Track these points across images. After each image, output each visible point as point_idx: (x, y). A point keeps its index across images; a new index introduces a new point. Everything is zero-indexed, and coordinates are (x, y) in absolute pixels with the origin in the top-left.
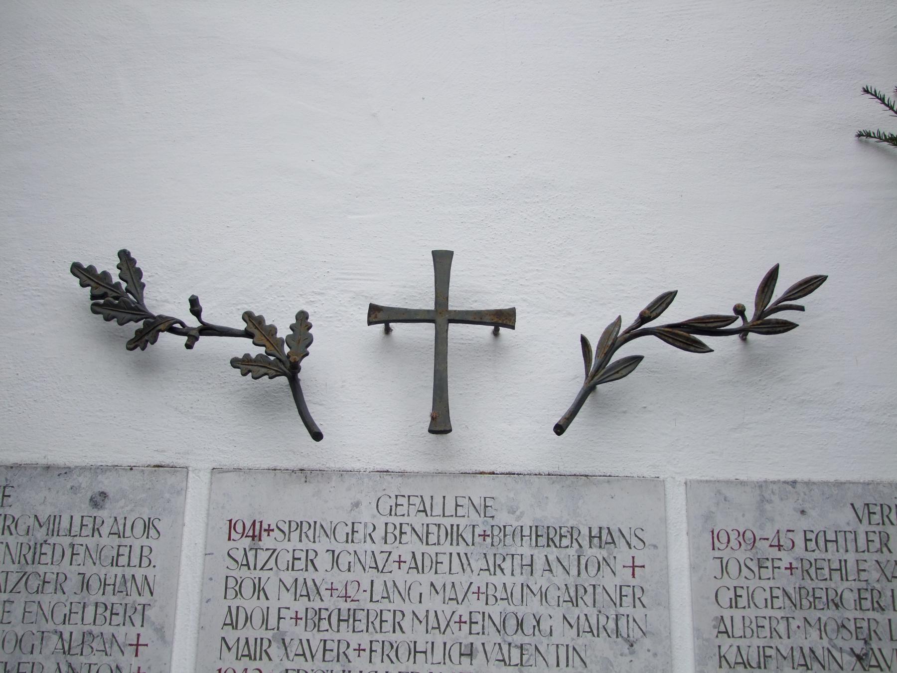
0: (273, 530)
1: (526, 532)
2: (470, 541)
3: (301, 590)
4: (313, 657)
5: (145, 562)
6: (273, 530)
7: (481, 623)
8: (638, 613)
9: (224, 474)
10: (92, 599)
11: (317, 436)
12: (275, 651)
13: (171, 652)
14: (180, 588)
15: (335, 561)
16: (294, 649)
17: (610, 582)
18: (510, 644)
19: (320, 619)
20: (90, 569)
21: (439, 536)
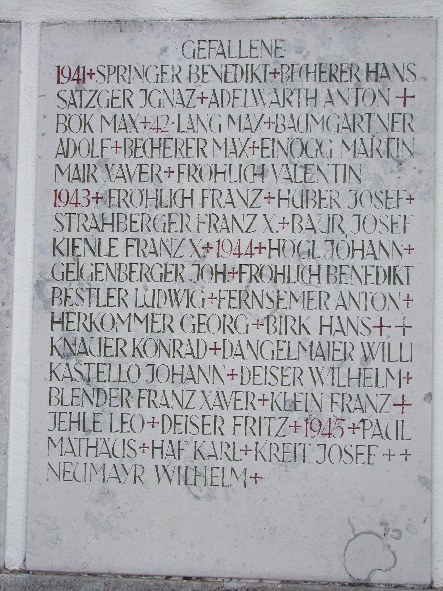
0: (94, 74)
1: (312, 69)
2: (262, 78)
4: (131, 179)
6: (94, 74)
7: (271, 148)
8: (407, 137)
9: (52, 27)
12: (100, 174)
13: (16, 178)
14: (20, 124)
15: (148, 99)
16: (115, 173)
18: (295, 165)
19: (136, 147)
21: (235, 75)
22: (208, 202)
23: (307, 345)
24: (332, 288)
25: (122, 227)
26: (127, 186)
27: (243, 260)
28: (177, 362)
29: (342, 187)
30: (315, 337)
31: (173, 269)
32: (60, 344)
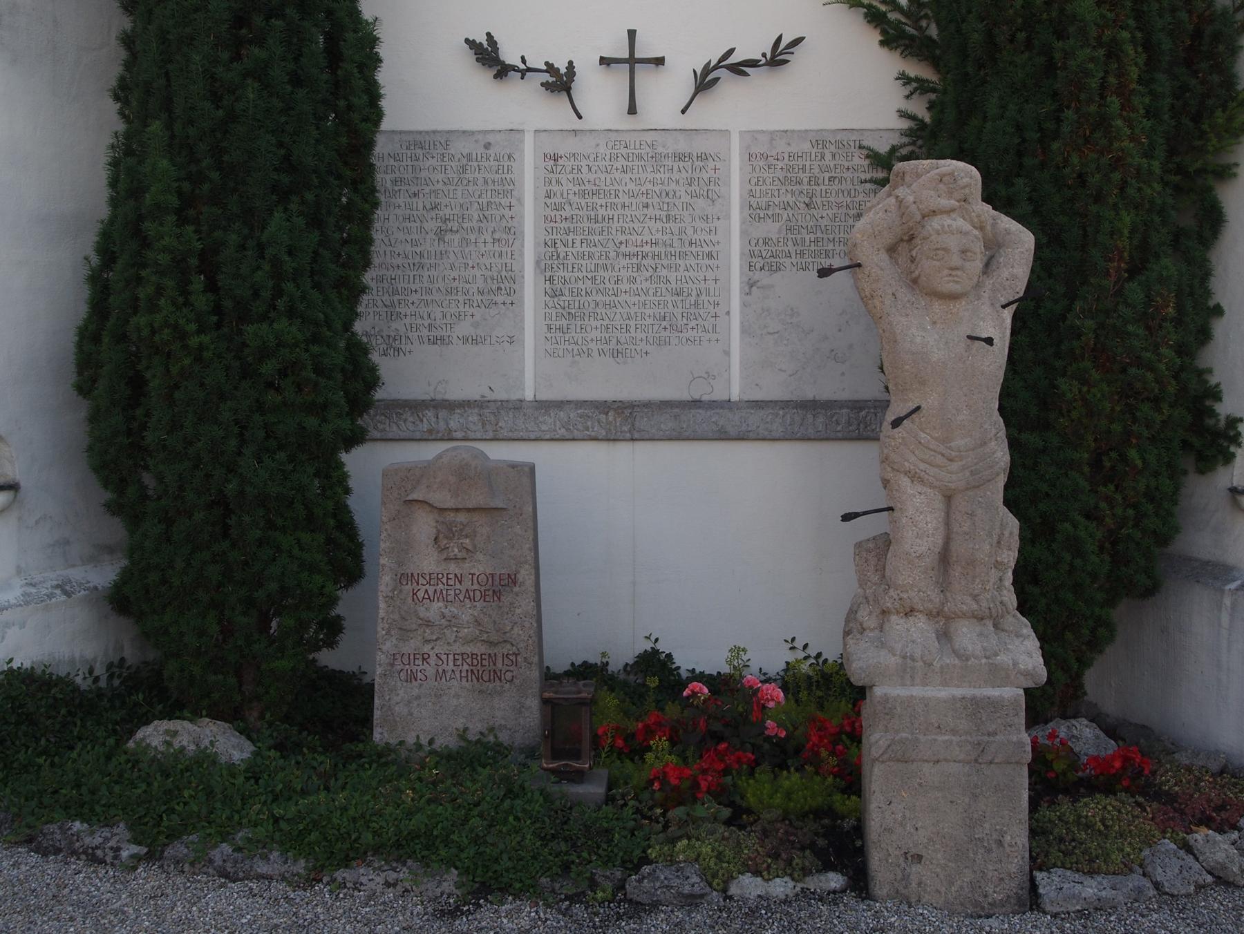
3: (576, 182)
5: (510, 172)
8: (717, 188)
10: (489, 188)
11: (580, 117)
17: (705, 176)
20: (487, 176)
22: (621, 220)
23: (670, 289)
24: (681, 262)
25: (578, 233)
26: (581, 213)
27: (638, 249)
28: (608, 299)
29: (686, 213)
30: (674, 285)
31: (604, 254)
32: (549, 291)
